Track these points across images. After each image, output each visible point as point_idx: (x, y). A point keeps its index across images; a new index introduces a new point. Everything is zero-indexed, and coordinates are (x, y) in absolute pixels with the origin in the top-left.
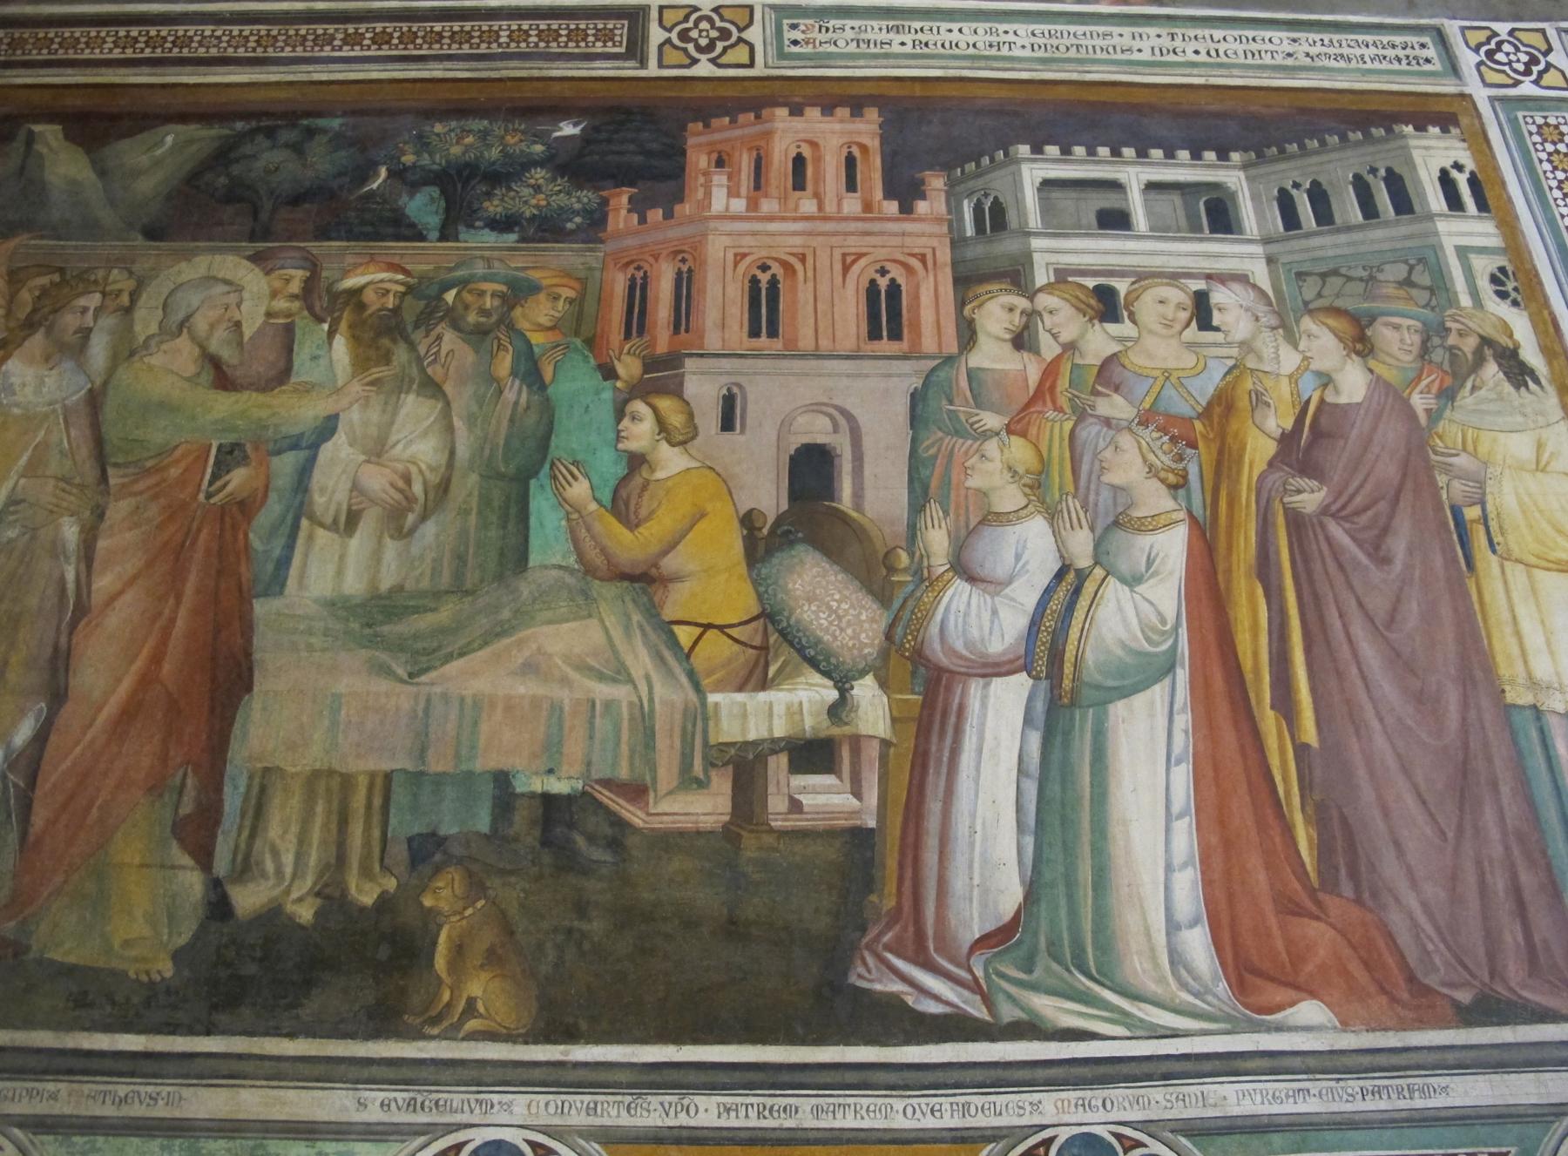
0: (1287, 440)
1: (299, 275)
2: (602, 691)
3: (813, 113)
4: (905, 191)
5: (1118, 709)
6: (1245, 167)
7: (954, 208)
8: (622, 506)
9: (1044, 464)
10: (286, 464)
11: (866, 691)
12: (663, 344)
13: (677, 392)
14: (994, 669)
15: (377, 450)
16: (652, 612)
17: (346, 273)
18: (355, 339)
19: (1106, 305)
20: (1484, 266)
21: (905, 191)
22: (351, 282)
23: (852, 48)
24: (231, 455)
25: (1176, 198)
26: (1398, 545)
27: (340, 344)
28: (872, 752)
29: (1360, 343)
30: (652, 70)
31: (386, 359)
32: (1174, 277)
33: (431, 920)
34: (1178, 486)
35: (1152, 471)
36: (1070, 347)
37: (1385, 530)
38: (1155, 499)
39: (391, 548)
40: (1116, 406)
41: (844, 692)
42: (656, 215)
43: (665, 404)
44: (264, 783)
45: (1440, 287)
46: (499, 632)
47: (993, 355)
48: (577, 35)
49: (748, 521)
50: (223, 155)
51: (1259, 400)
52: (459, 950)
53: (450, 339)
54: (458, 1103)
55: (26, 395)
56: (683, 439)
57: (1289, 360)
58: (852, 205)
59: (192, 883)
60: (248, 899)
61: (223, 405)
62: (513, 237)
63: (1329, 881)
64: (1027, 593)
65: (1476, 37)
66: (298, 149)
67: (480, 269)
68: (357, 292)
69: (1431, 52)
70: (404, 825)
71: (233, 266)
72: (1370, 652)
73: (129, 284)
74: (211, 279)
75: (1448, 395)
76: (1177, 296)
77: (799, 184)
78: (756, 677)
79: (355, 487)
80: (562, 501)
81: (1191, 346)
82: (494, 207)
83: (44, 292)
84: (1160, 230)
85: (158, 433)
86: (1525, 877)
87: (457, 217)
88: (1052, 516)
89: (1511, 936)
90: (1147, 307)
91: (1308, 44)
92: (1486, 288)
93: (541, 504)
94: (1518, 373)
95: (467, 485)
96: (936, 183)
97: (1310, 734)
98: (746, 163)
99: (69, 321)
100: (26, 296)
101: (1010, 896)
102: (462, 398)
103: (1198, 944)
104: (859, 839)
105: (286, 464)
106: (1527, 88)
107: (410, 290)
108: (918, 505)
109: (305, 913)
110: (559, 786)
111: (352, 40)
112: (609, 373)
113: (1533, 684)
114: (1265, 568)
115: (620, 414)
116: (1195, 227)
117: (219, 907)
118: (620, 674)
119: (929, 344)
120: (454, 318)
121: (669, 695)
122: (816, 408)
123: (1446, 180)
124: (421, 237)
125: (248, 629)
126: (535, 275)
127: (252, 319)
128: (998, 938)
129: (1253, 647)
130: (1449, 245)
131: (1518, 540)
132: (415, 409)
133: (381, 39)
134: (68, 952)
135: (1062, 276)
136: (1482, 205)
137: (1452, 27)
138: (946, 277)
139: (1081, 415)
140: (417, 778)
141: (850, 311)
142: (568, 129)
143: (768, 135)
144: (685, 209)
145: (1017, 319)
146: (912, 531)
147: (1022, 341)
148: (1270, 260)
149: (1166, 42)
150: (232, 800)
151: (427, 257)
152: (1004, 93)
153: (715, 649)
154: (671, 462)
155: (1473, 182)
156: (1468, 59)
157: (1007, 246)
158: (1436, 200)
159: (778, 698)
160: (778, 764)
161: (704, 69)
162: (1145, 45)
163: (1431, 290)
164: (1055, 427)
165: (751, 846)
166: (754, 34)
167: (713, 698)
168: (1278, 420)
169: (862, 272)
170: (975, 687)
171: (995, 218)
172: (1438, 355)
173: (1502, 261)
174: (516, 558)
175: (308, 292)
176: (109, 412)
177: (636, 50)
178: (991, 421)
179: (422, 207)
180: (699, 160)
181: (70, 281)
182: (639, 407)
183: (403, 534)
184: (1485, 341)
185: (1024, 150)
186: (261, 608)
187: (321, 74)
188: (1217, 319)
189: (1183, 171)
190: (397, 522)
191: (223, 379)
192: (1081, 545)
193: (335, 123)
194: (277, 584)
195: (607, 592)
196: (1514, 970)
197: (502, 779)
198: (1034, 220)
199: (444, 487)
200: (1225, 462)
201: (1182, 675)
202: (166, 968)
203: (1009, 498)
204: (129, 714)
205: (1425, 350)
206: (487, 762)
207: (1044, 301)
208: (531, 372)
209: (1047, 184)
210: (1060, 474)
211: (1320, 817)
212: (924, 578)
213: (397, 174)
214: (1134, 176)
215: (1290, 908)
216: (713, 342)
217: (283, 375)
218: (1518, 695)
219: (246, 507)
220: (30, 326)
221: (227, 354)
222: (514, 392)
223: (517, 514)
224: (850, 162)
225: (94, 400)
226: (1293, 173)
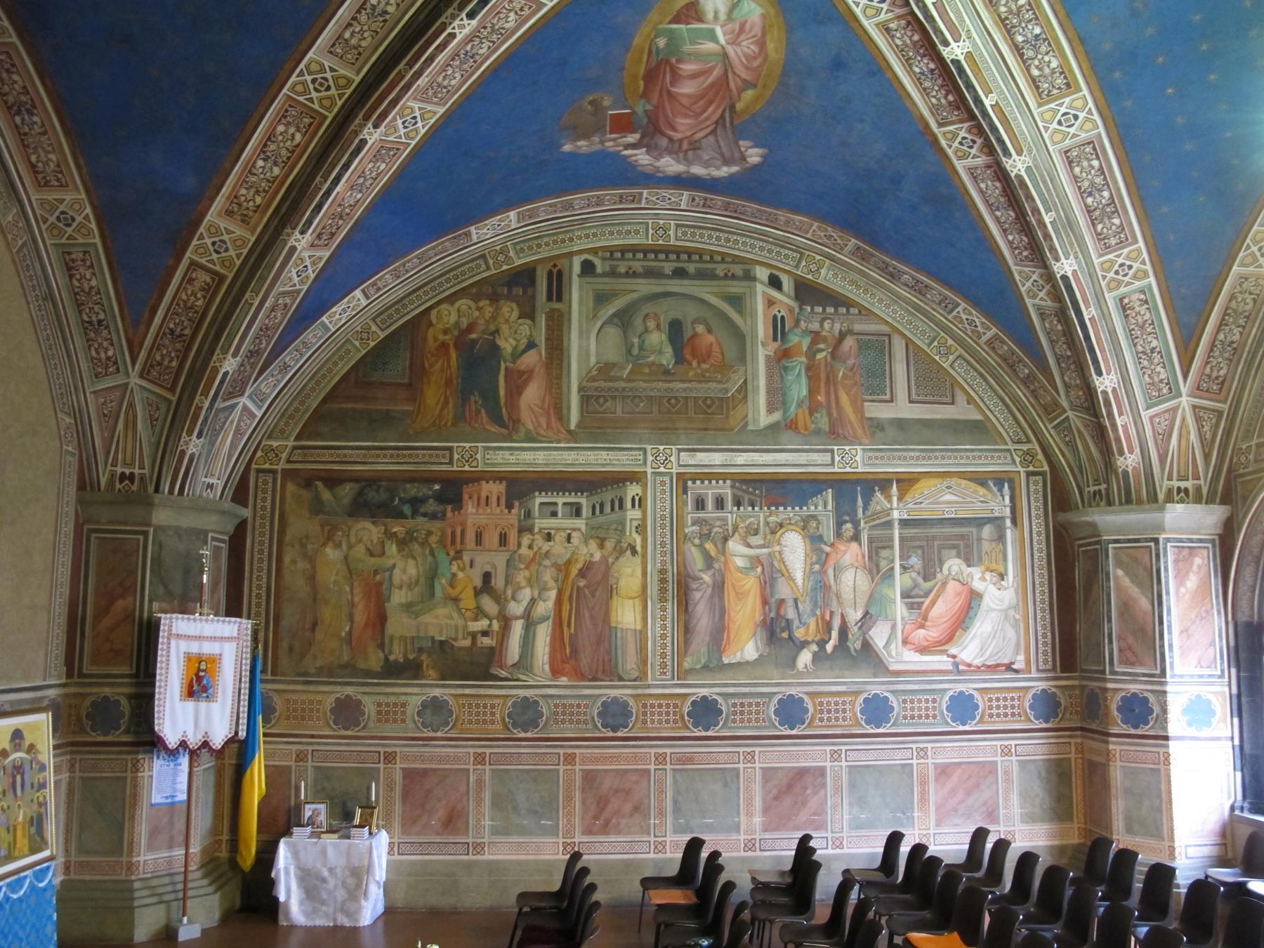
0: (581, 570)
1: (383, 528)
2: (449, 621)
3: (491, 482)
4: (510, 507)
5: (539, 626)
6: (587, 497)
7: (520, 511)
8: (452, 585)
9: (531, 576)
10: (387, 574)
11: (495, 622)
12: (458, 548)
13: (460, 558)
14: (518, 618)
15: (404, 571)
16: (458, 606)
17: (393, 527)
18: (397, 545)
19: (549, 537)
20: (635, 523)
21: (510, 507)
22: (395, 530)
23: (501, 461)
24: (376, 572)
25: (568, 508)
26: (597, 594)
27: (394, 546)
28: (495, 634)
29: (601, 546)
30: (455, 469)
31: (403, 550)
32: (564, 530)
33: (422, 662)
34: (556, 581)
35: (552, 578)
36: (540, 548)
37: (596, 590)
38: (552, 584)
39: (409, 593)
40: (547, 562)
41: (491, 621)
42: (456, 513)
43: (459, 562)
44: (392, 638)
45: (623, 531)
46: (432, 610)
47: (524, 551)
48: (437, 456)
49: (475, 588)
50: (361, 493)
51: (577, 561)
52: (427, 666)
53: (416, 546)
54: (428, 690)
55: (332, 557)
56: (462, 569)
57: (585, 550)
58: (498, 511)
59: (382, 655)
60: (392, 658)
61: (373, 560)
62: (426, 519)
63: (571, 658)
64: (525, 603)
65: (655, 451)
66: (377, 491)
67: (420, 527)
68: (395, 533)
69: (641, 458)
70: (417, 645)
71: (367, 524)
72: (587, 614)
73: (346, 529)
74: (364, 529)
75: (617, 559)
76: (564, 534)
77: (487, 505)
78: (476, 619)
79: (401, 580)
80: (440, 583)
81: (565, 548)
82: (422, 510)
83: (330, 531)
84: (564, 516)
85: (360, 566)
86: (606, 658)
87: (415, 513)
88: (531, 587)
89: (601, 668)
90: (557, 538)
91: (611, 456)
92: (634, 529)
93: (436, 584)
94: (634, 552)
95: (422, 580)
96: (517, 504)
97: (572, 631)
98: (475, 497)
99: (336, 538)
100: (326, 531)
101: (516, 658)
102: (420, 560)
103: (547, 667)
104: (492, 648)
105: (387, 574)
106: (662, 469)
107: (407, 533)
108: (506, 585)
109: (402, 660)
110: (443, 639)
111: (385, 456)
112: (448, 554)
113: (617, 622)
114: (570, 598)
115: (451, 563)
116: (571, 516)
117: (387, 659)
118: (451, 618)
119: (511, 548)
120: (416, 539)
121: (461, 622)
122: (488, 563)
123: (633, 500)
124: (407, 518)
125: (385, 609)
126: (433, 529)
127: (375, 538)
128: (514, 665)
129: (565, 615)
130: (629, 518)
131: (623, 592)
132: (411, 563)
133: (392, 456)
134: (362, 666)
135: (541, 529)
136: (640, 506)
137: (649, 447)
138: (516, 530)
139: (540, 565)
140: (418, 637)
141: (496, 539)
142: (437, 487)
143: (481, 489)
144: (462, 511)
145: (529, 542)
146: (505, 592)
147: (530, 547)
148: (587, 524)
149: (575, 457)
150: (387, 641)
151: (410, 523)
152: (535, 475)
153: (468, 614)
154: (461, 575)
155: (640, 500)
156: (650, 458)
157: (530, 522)
158: (629, 505)
159: (479, 623)
160: (479, 635)
161: (467, 468)
162: (570, 458)
163: (621, 531)
164: (534, 567)
165: (474, 649)
166: (478, 456)
167: (469, 623)
168: (579, 565)
169: (499, 530)
170: (514, 622)
171: (528, 514)
172: (618, 548)
173: (639, 522)
174: (432, 595)
175: (385, 533)
176: (349, 560)
177: (451, 462)
178: (522, 566)
179: (407, 509)
180: (466, 497)
181: (334, 529)
182: (454, 562)
183: (411, 590)
184: (629, 544)
185: (537, 493)
186: (386, 604)
187: (380, 467)
188: (572, 540)
189: (572, 499)
190: (410, 587)
191: (372, 555)
192: (536, 593)
193: (384, 484)
194: (389, 600)
195: (450, 604)
196: (600, 674)
197: (433, 638)
198: (537, 514)
199: (417, 581)
200: (566, 576)
201: (551, 620)
202: (379, 669)
203: (524, 583)
204: (366, 625)
205: (615, 547)
206: (431, 634)
207: (537, 536)
208: (432, 553)
209: (541, 504)
210: (534, 578)
211: (571, 645)
212: (506, 600)
213: (401, 500)
214: (560, 500)
215: (563, 662)
216: (469, 547)
217: (383, 554)
218: (613, 624)
219: (380, 584)
220: (328, 539)
221: (371, 548)
222: (430, 559)
223: (432, 587)
224: (498, 498)
225: (346, 558)
226: (597, 499)
